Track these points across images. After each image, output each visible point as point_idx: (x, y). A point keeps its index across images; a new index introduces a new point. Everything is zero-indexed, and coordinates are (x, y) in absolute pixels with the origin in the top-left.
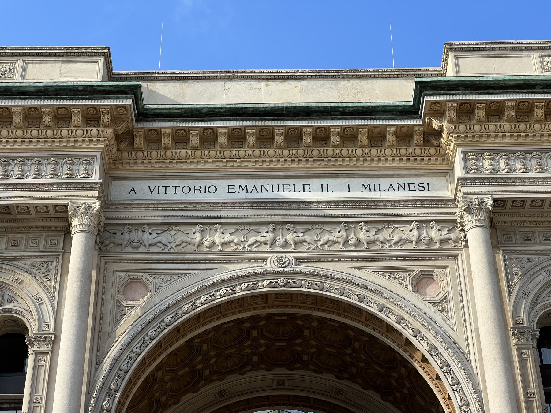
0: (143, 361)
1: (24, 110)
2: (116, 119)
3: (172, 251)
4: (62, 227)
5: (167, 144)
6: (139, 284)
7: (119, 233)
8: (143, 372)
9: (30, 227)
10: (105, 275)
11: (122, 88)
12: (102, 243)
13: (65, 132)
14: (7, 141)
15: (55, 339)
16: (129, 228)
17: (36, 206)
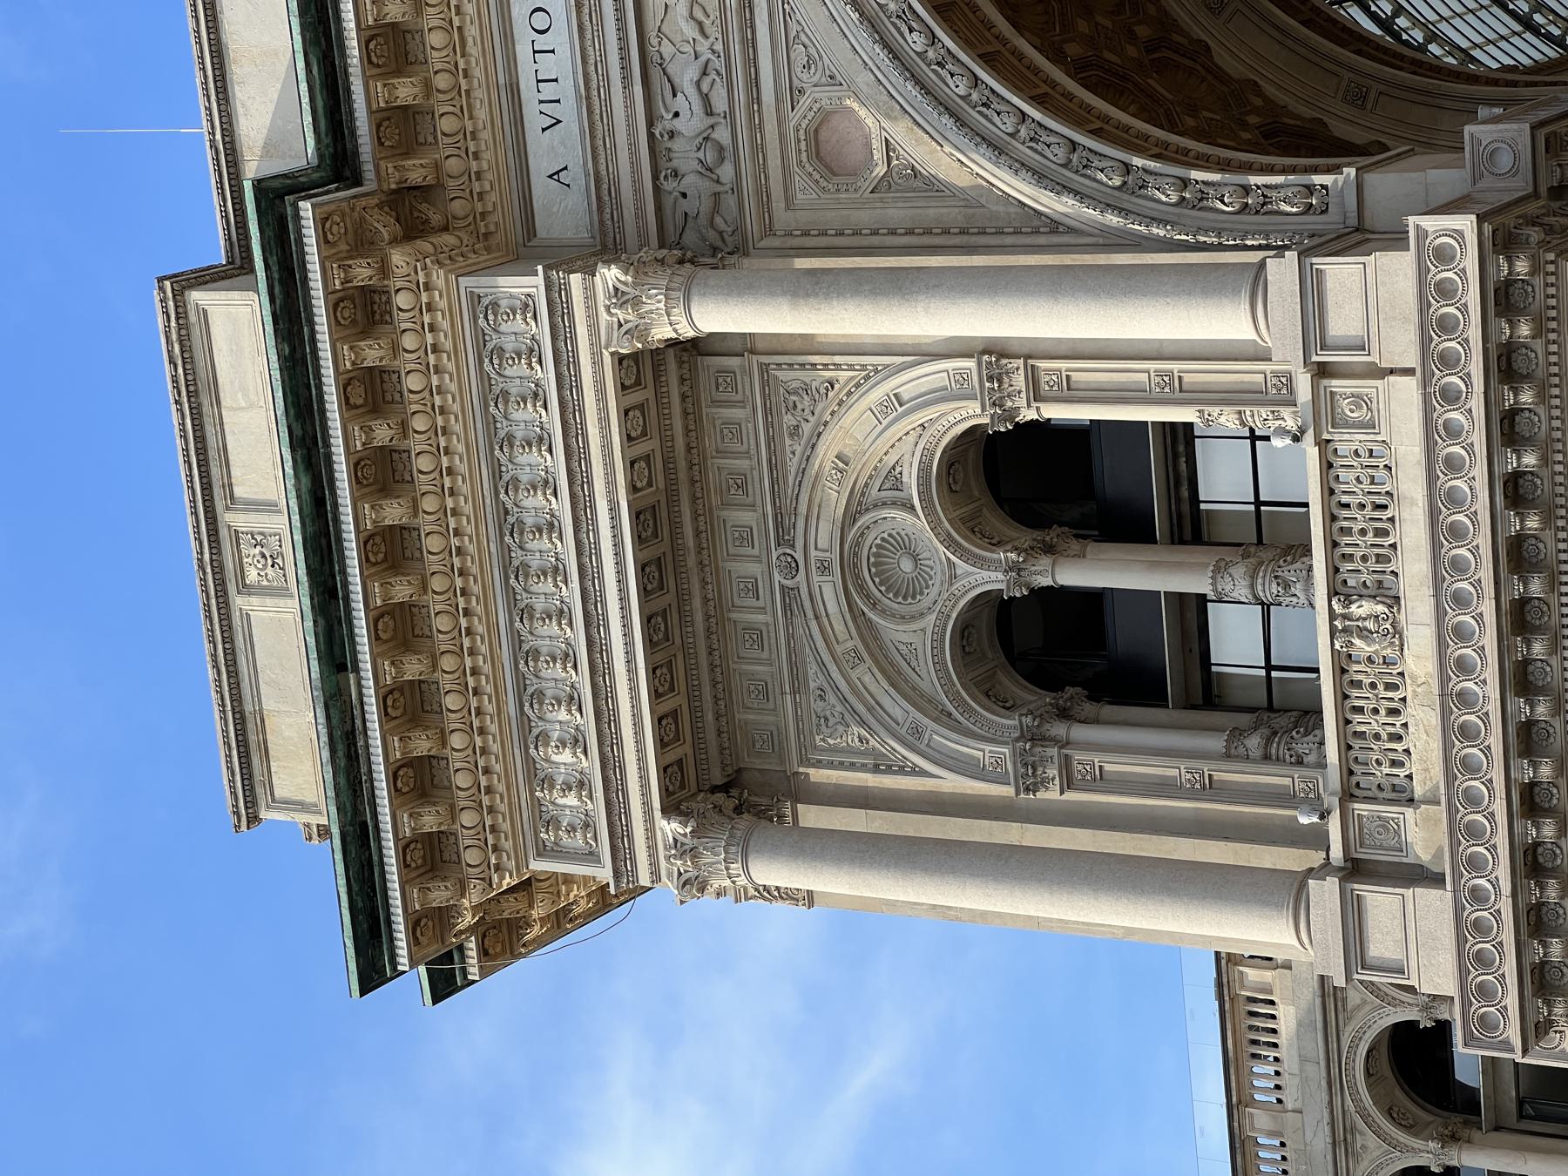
0: (1039, 101)
1: (363, 497)
2: (362, 243)
3: (719, 47)
4: (681, 363)
5: (416, 90)
6: (823, 135)
7: (684, 205)
8: (1070, 97)
9: (689, 449)
10: (806, 234)
11: (269, 233)
12: (715, 250)
13: (413, 382)
14: (457, 533)
15: (994, 353)
16: (666, 177)
17: (629, 439)
